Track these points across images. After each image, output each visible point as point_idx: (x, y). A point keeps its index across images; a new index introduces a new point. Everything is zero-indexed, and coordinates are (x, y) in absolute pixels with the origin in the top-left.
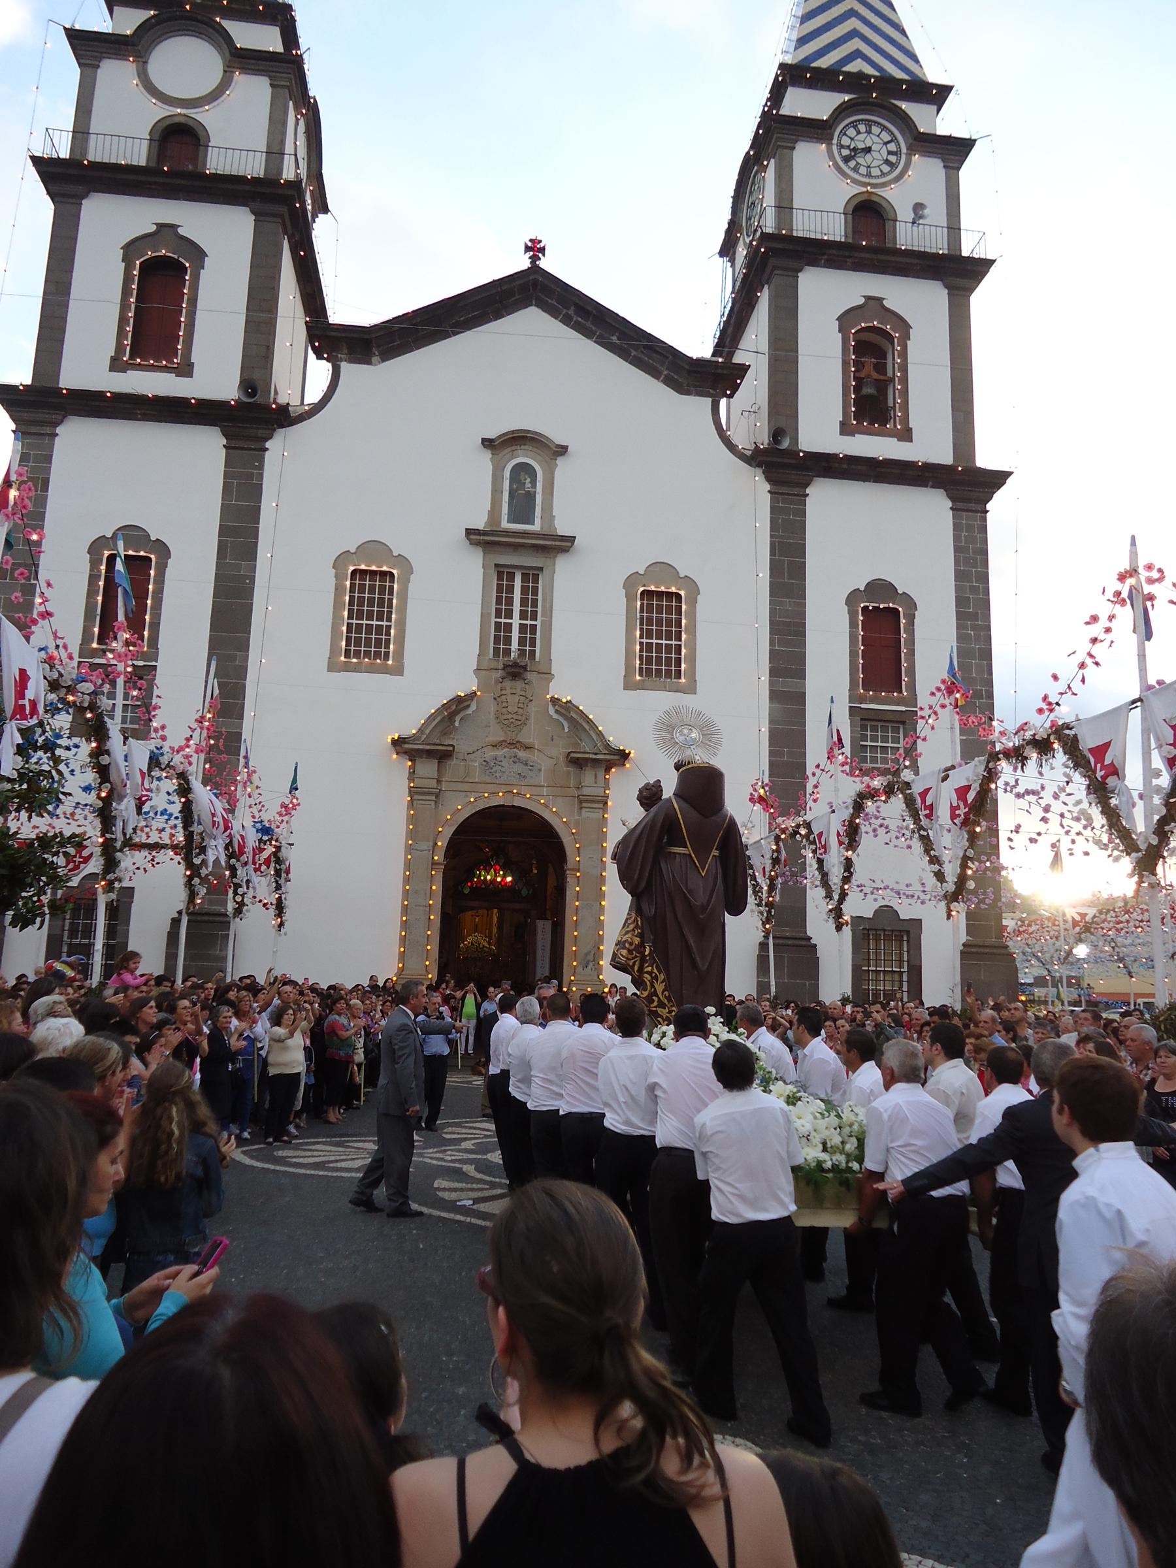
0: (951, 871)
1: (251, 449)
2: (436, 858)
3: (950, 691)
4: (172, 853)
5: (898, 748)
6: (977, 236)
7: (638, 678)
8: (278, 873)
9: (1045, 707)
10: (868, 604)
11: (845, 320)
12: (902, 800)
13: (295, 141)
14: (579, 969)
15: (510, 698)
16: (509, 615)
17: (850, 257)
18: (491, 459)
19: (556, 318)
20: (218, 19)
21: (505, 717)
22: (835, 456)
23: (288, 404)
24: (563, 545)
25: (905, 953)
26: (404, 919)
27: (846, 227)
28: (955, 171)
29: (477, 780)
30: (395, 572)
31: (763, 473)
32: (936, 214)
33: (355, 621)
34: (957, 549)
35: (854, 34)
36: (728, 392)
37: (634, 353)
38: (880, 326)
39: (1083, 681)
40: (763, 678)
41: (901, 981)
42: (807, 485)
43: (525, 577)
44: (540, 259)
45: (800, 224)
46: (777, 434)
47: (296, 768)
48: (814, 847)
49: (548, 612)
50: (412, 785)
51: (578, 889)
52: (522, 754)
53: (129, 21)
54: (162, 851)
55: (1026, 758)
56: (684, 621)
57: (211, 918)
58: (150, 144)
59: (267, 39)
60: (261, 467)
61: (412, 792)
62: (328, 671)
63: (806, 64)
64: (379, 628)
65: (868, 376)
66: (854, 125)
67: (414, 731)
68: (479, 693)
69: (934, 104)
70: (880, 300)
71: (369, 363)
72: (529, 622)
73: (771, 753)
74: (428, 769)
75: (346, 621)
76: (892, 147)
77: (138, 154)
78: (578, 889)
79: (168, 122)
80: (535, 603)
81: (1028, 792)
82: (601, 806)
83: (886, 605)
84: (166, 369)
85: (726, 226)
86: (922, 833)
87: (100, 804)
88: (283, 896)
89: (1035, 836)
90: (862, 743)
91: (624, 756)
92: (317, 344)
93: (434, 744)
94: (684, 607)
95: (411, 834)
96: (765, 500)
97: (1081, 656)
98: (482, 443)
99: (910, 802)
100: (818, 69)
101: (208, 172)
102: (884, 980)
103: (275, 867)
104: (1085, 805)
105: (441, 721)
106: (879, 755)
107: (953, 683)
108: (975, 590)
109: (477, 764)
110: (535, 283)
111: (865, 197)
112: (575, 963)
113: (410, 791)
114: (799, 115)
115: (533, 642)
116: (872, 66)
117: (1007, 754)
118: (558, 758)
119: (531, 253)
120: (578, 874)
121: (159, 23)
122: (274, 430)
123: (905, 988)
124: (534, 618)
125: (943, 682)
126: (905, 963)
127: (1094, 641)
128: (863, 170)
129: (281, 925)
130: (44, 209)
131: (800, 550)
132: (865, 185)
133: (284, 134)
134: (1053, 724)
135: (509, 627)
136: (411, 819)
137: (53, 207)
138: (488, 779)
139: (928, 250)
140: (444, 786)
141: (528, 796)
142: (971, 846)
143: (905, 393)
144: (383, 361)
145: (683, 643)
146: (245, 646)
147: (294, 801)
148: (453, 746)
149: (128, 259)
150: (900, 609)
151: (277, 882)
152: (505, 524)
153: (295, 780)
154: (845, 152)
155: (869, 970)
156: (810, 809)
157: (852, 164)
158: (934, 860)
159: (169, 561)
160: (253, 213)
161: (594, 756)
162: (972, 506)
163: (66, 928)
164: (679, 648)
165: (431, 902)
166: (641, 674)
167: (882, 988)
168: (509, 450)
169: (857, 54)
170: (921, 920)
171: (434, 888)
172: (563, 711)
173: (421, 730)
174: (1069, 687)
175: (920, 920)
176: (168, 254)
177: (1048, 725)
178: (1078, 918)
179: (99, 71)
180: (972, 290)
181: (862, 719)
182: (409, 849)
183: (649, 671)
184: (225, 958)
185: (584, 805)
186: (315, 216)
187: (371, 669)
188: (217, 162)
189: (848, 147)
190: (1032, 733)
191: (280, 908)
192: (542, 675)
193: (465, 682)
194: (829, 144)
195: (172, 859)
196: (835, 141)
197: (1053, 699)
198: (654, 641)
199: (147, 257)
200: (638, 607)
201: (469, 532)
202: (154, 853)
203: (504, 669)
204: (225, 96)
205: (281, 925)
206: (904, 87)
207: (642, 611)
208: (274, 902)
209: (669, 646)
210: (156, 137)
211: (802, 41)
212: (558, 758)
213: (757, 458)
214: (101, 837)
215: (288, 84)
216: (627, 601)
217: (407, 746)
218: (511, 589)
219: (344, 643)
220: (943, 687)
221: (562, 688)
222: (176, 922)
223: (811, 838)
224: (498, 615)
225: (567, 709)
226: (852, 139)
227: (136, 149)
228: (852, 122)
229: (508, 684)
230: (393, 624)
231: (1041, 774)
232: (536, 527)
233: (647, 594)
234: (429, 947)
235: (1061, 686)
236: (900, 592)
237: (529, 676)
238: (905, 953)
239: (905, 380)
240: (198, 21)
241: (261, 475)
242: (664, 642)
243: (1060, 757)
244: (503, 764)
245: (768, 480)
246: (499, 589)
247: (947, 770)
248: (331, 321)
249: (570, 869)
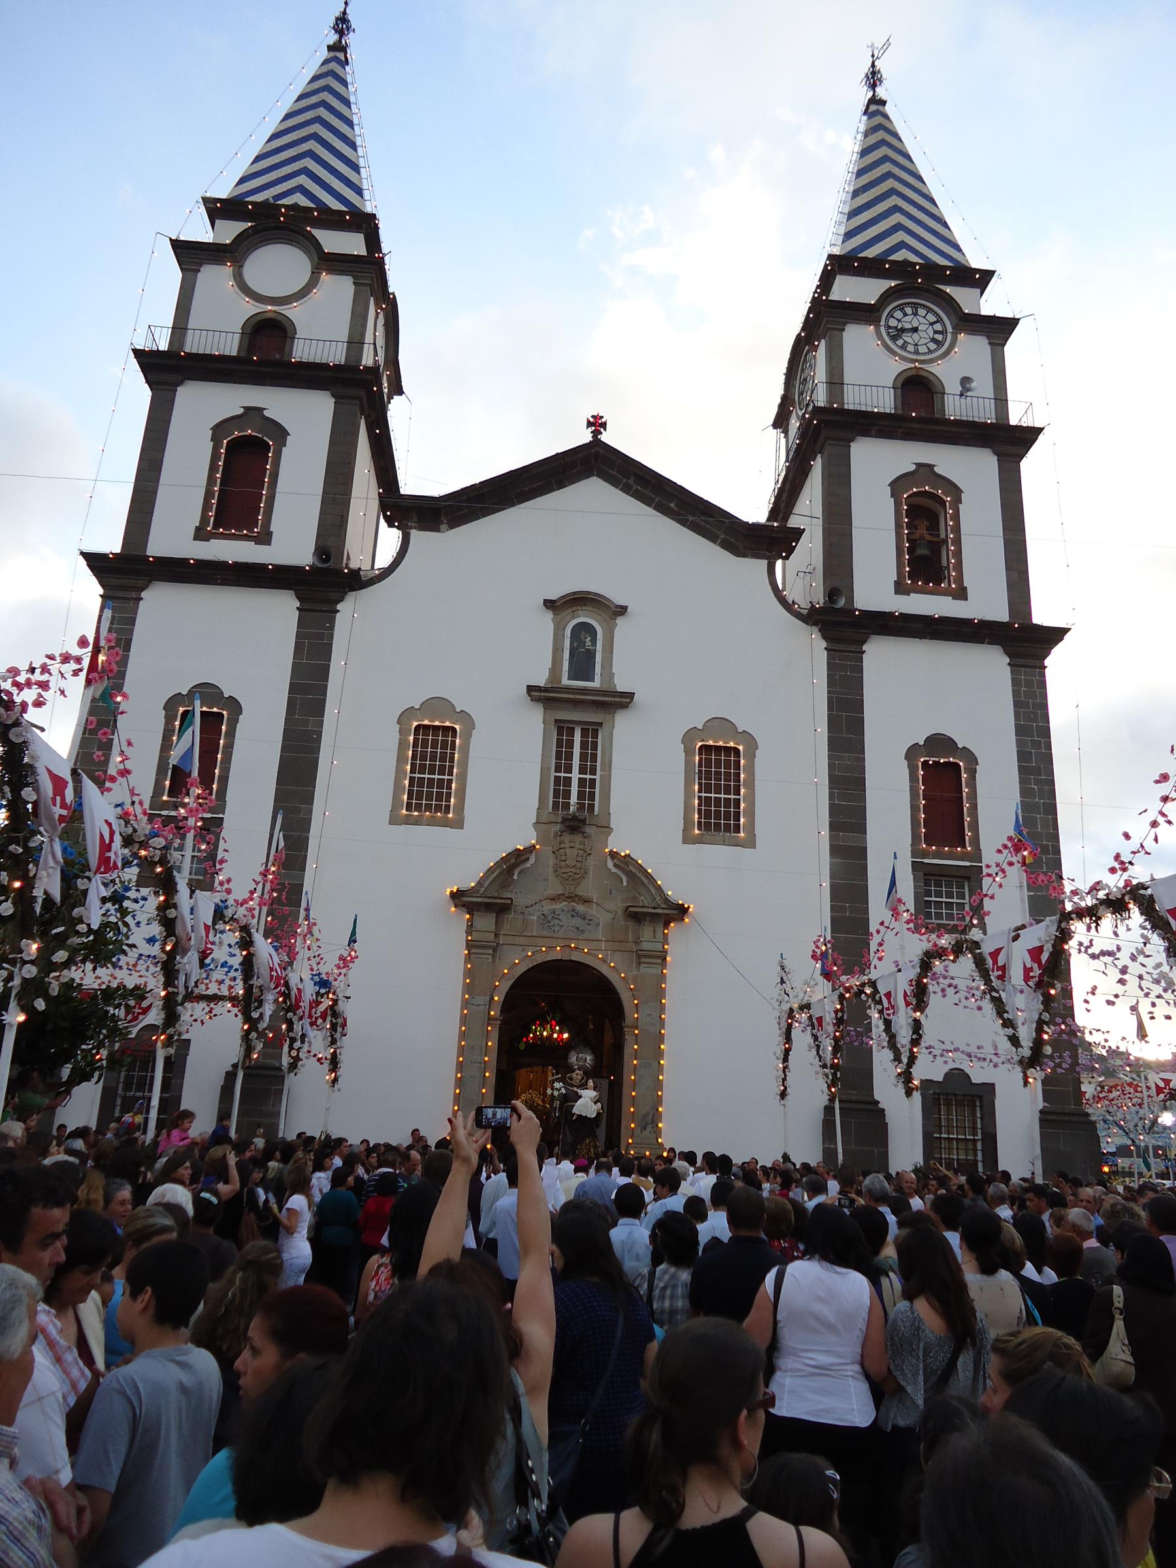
0: (1026, 1034)
1: (324, 611)
2: (492, 1013)
3: (1017, 848)
4: (229, 1005)
5: (964, 904)
6: (1024, 407)
7: (697, 832)
8: (334, 1027)
9: (1117, 866)
10: (928, 759)
11: (897, 485)
12: (972, 961)
13: (374, 332)
14: (638, 1132)
15: (568, 851)
16: (569, 769)
17: (900, 427)
18: (553, 620)
19: (617, 487)
20: (308, 229)
21: (564, 870)
22: (891, 614)
23: (360, 569)
24: (624, 700)
25: (979, 1121)
26: (459, 1075)
27: (895, 401)
28: (1000, 348)
30: (457, 727)
31: (820, 631)
32: (983, 386)
33: (417, 775)
34: (1017, 704)
35: (898, 227)
36: (784, 554)
37: (691, 518)
38: (932, 490)
39: (1156, 840)
40: (823, 833)
41: (975, 1150)
42: (864, 642)
43: (585, 733)
44: (601, 433)
45: (851, 395)
46: (832, 594)
47: (355, 920)
48: (880, 1007)
49: (608, 766)
50: (470, 938)
51: (636, 1047)
52: (581, 908)
53: (229, 231)
54: (221, 1002)
55: (1100, 918)
56: (742, 776)
57: (266, 1072)
58: (242, 337)
59: (352, 244)
60: (332, 627)
61: (469, 945)
62: (390, 824)
63: (854, 254)
64: (441, 781)
65: (922, 538)
66: (901, 308)
67: (473, 884)
68: (538, 847)
69: (978, 288)
70: (930, 467)
71: (438, 530)
72: (588, 777)
73: (832, 908)
74: (486, 922)
75: (408, 774)
76: (938, 327)
77: (230, 346)
78: (636, 1047)
79: (259, 318)
80: (594, 758)
81: (1103, 953)
82: (660, 961)
83: (947, 760)
84: (246, 538)
85: (779, 401)
86: (994, 994)
87: (165, 957)
88: (338, 1051)
89: (1112, 998)
90: (926, 899)
91: (682, 911)
92: (388, 513)
93: (493, 897)
94: (742, 762)
95: (468, 988)
96: (821, 657)
97: (1152, 815)
98: (544, 604)
99: (979, 962)
100: (866, 258)
101: (293, 360)
102: (957, 1149)
103: (331, 1021)
104: (1165, 968)
105: (500, 874)
106: (944, 911)
107: (1020, 840)
108: (1037, 745)
110: (597, 455)
111: (914, 372)
113: (467, 944)
114: (848, 300)
115: (592, 796)
116: (916, 255)
117: (1080, 913)
118: (616, 912)
119: (593, 428)
120: (636, 1032)
121: (255, 233)
122: (346, 593)
123: (980, 1154)
124: (593, 772)
125: (1010, 839)
126: (979, 1131)
127: (1165, 799)
128: (911, 348)
129: (335, 1080)
130: (141, 395)
131: (857, 706)
132: (915, 361)
133: (364, 326)
134: (1127, 883)
135: (568, 781)
136: (468, 973)
137: (150, 393)
138: (545, 933)
139: (976, 420)
141: (586, 950)
142: (1046, 1009)
143: (958, 553)
144: (451, 527)
145: (741, 797)
146: (310, 799)
147: (353, 953)
148: (512, 899)
149: (216, 439)
150: (961, 764)
151: (332, 1036)
152: (565, 681)
153: (354, 933)
154: (893, 332)
155: (940, 1137)
156: (875, 968)
157: (900, 342)
158: (1008, 1024)
159: (241, 717)
160: (333, 396)
161: (653, 911)
162: (1029, 662)
163: (122, 1080)
164: (737, 802)
165: (486, 1059)
167: (955, 1157)
168: (569, 611)
169: (902, 245)
170: (994, 1084)
171: (490, 1044)
172: (622, 865)
173: (480, 883)
174: (1142, 846)
175: (994, 1084)
176: (253, 434)
177: (1121, 884)
178: (1162, 1084)
179: (199, 274)
181: (925, 874)
182: (465, 1004)
183: (707, 827)
184: (278, 1114)
185: (643, 960)
186: (390, 397)
187: (432, 822)
188: (302, 352)
189: (896, 328)
190: (1107, 891)
191: (334, 1063)
192: (601, 829)
193: (524, 836)
194: (877, 326)
195: (229, 1011)
196: (882, 323)
197: (1125, 858)
198: (713, 795)
199: (234, 436)
200: (697, 761)
201: (530, 689)
202: (212, 1005)
203: (563, 822)
204: (312, 294)
205: (335, 1080)
206: (948, 273)
207: (700, 765)
208: (329, 1057)
209: (727, 801)
210: (248, 331)
211: (849, 235)
212: (616, 912)
213: (812, 617)
214: (164, 990)
215: (370, 282)
216: (686, 755)
217: (465, 899)
218: (570, 744)
219: (406, 797)
220: (1009, 845)
221: (621, 842)
222: (230, 1076)
223: (877, 997)
224: (558, 770)
225: (626, 863)
226: (899, 321)
227: (229, 342)
228: (899, 305)
229: (567, 838)
230: (454, 778)
231: (1116, 934)
232: (596, 684)
233: (706, 749)
235: (1134, 844)
236: (960, 746)
237: (588, 829)
238: (979, 1121)
239: (958, 542)
240: (291, 231)
241: (331, 636)
242: (722, 796)
243: (1136, 917)
244: (560, 917)
245: (825, 637)
246: (559, 744)
247: (1017, 929)
248: (402, 492)
249: (628, 1027)
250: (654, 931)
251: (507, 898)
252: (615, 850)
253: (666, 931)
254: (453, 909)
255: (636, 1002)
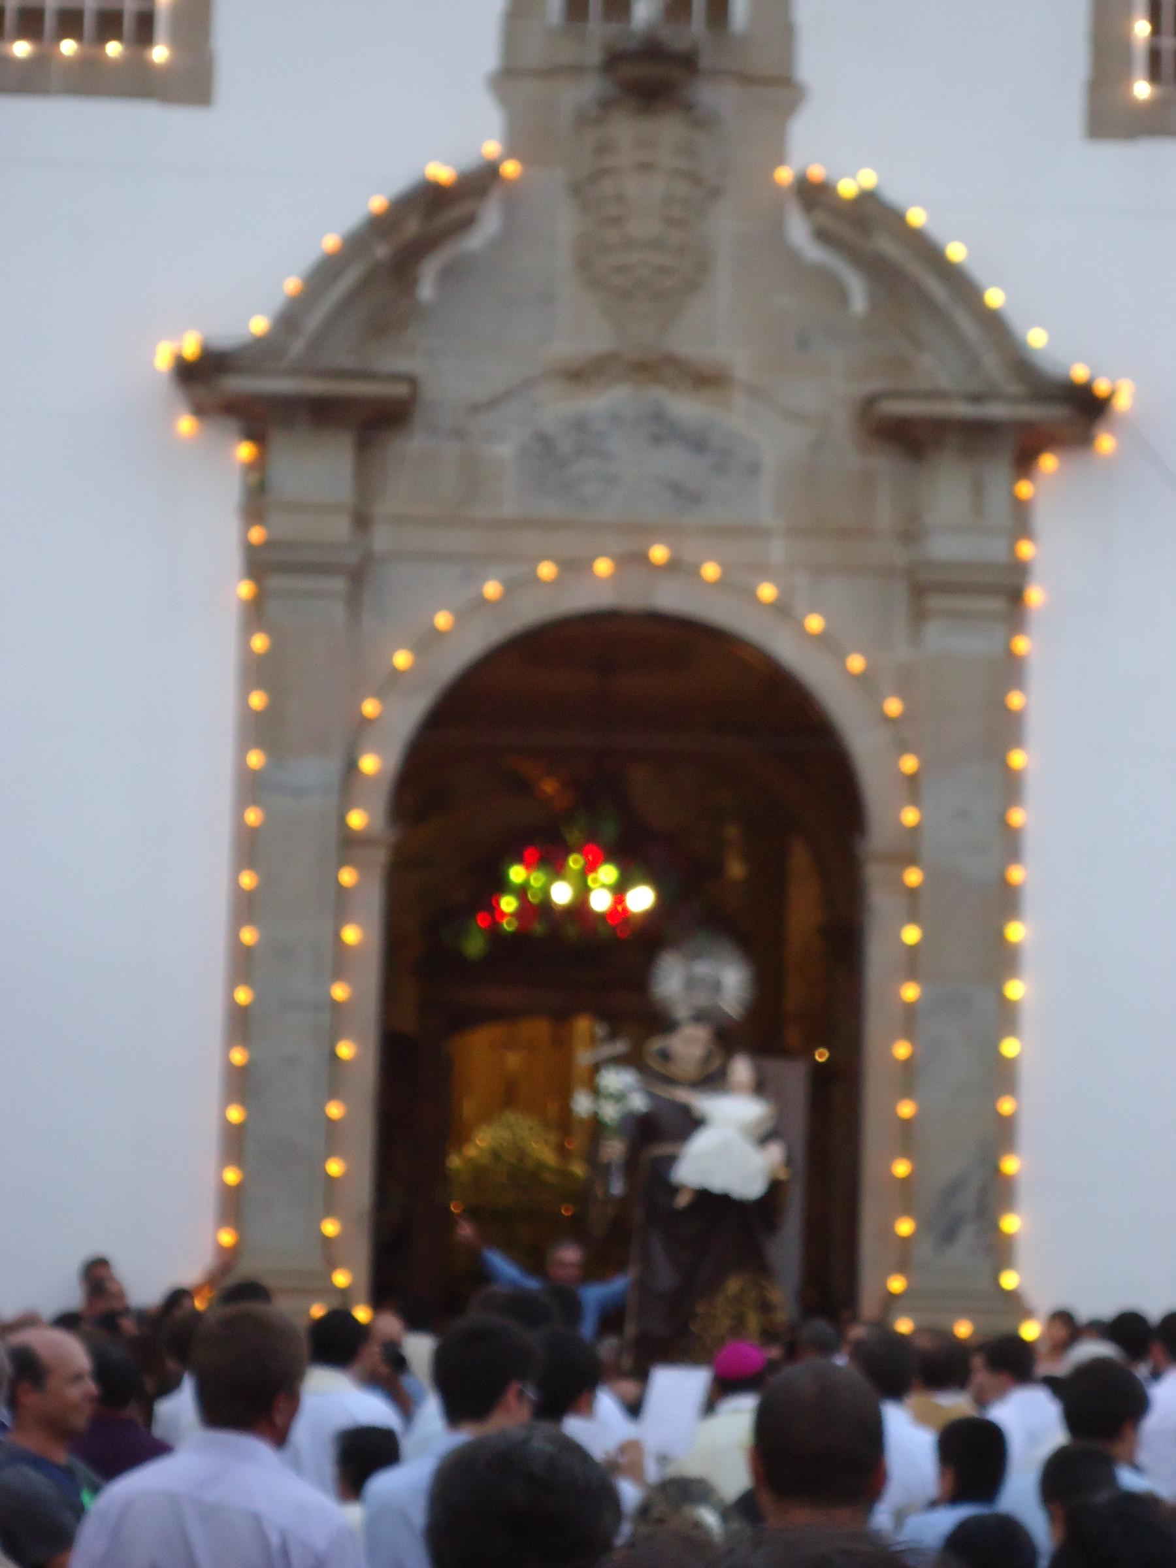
2: (356, 820)
7: (1142, 90)
26: (238, 1056)
29: (508, 510)
50: (257, 534)
67: (259, 325)
68: (510, 168)
78: (911, 935)
82: (997, 604)
109: (505, 450)
112: (905, 1227)
120: (913, 877)
140: (382, 539)
141: (711, 571)
148: (412, 380)
166: (1155, 74)
185: (935, 602)
234: (334, 1168)
250: (978, 490)
251: (396, 377)
252: (817, 172)
253: (1025, 489)
254: (186, 424)
255: (909, 764)
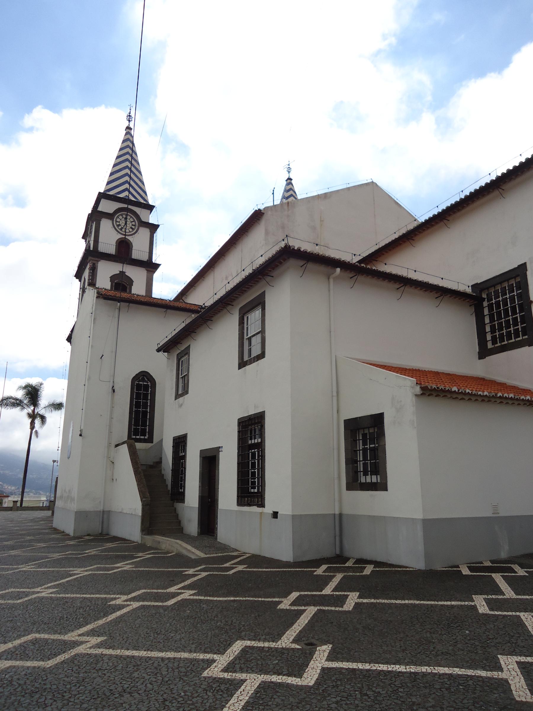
66: (122, 215)
76: (133, 223)
154: (118, 223)
180: (154, 272)
196: (115, 220)
226: (121, 219)
